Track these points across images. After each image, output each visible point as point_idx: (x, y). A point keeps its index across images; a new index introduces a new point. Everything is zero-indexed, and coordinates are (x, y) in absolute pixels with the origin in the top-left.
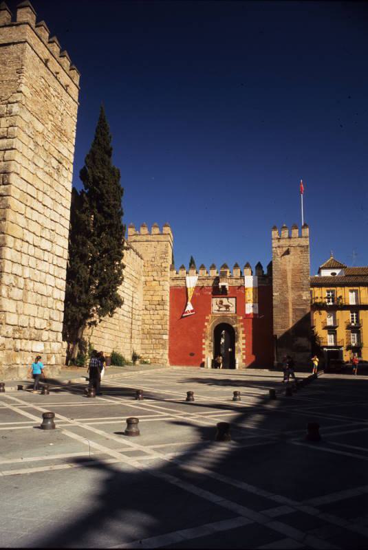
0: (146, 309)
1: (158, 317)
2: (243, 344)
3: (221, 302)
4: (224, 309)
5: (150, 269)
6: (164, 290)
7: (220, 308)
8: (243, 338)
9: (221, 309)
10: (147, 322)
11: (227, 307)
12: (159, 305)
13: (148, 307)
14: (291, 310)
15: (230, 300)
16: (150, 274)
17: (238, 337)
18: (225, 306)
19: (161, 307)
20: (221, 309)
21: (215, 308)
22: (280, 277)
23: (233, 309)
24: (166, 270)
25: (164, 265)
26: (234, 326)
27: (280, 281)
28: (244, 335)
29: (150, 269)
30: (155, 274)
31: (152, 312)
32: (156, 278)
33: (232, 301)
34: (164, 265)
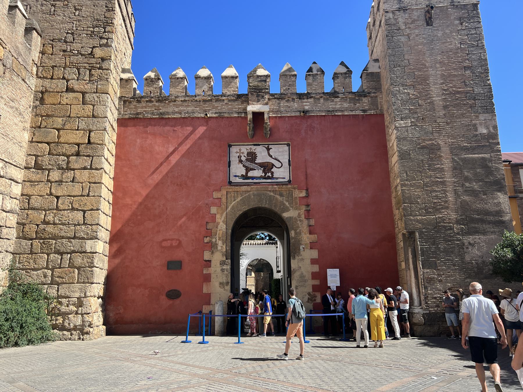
0: (38, 166)
1: (77, 190)
2: (313, 262)
3: (252, 157)
4: (258, 173)
5: (59, 59)
6: (94, 116)
7: (248, 169)
8: (312, 246)
9: (250, 174)
10: (36, 202)
11: (267, 167)
12: (78, 154)
13: (45, 161)
14: (447, 164)
15: (275, 150)
16: (58, 72)
17: (298, 243)
18: (262, 165)
19: (85, 162)
20: (250, 174)
21: (238, 170)
22: (409, 82)
23: (282, 173)
24: (105, 65)
25: (99, 52)
26: (285, 215)
27: (411, 91)
28: (314, 237)
29: (59, 59)
30: (71, 74)
31: (55, 175)
32: (74, 84)
33: (281, 153)
34: (99, 52)
